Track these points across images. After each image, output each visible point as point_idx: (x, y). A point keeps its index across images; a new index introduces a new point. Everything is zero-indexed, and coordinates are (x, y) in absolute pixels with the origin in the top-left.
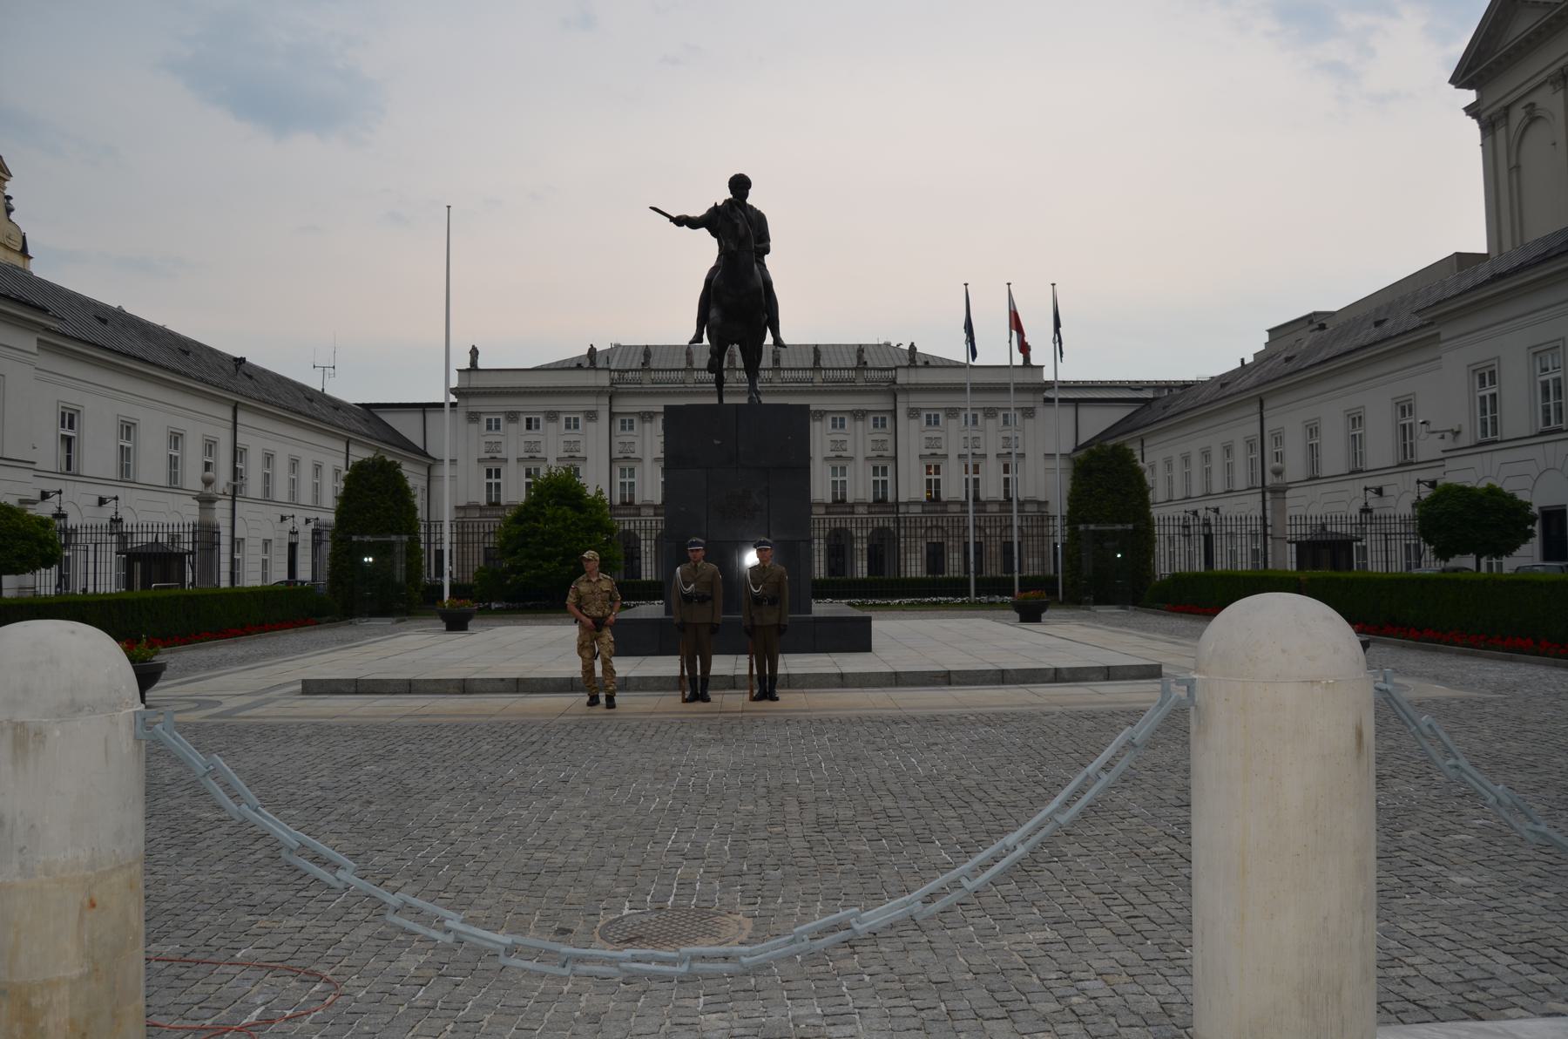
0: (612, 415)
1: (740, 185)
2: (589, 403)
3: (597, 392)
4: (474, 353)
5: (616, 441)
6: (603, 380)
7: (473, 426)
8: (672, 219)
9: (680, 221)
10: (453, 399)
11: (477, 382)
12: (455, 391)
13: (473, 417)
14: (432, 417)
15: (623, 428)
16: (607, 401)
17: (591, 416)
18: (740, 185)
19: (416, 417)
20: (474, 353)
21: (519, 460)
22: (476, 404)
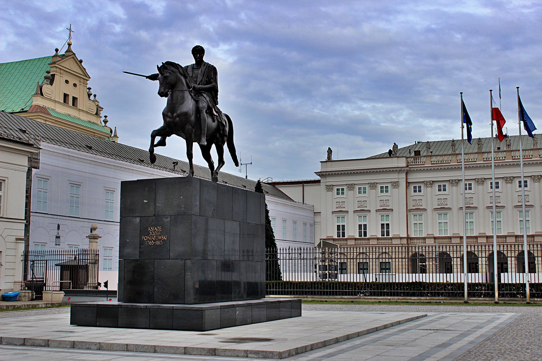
0: (408, 184)
1: (198, 52)
2: (394, 177)
3: (398, 170)
4: (330, 151)
5: (410, 200)
6: (402, 163)
7: (330, 193)
8: (147, 77)
9: (153, 77)
10: (318, 178)
11: (331, 168)
12: (321, 174)
13: (329, 188)
14: (307, 188)
15: (415, 191)
16: (405, 174)
17: (396, 185)
18: (198, 52)
19: (299, 188)
20: (330, 151)
21: (355, 212)
22: (330, 181)
